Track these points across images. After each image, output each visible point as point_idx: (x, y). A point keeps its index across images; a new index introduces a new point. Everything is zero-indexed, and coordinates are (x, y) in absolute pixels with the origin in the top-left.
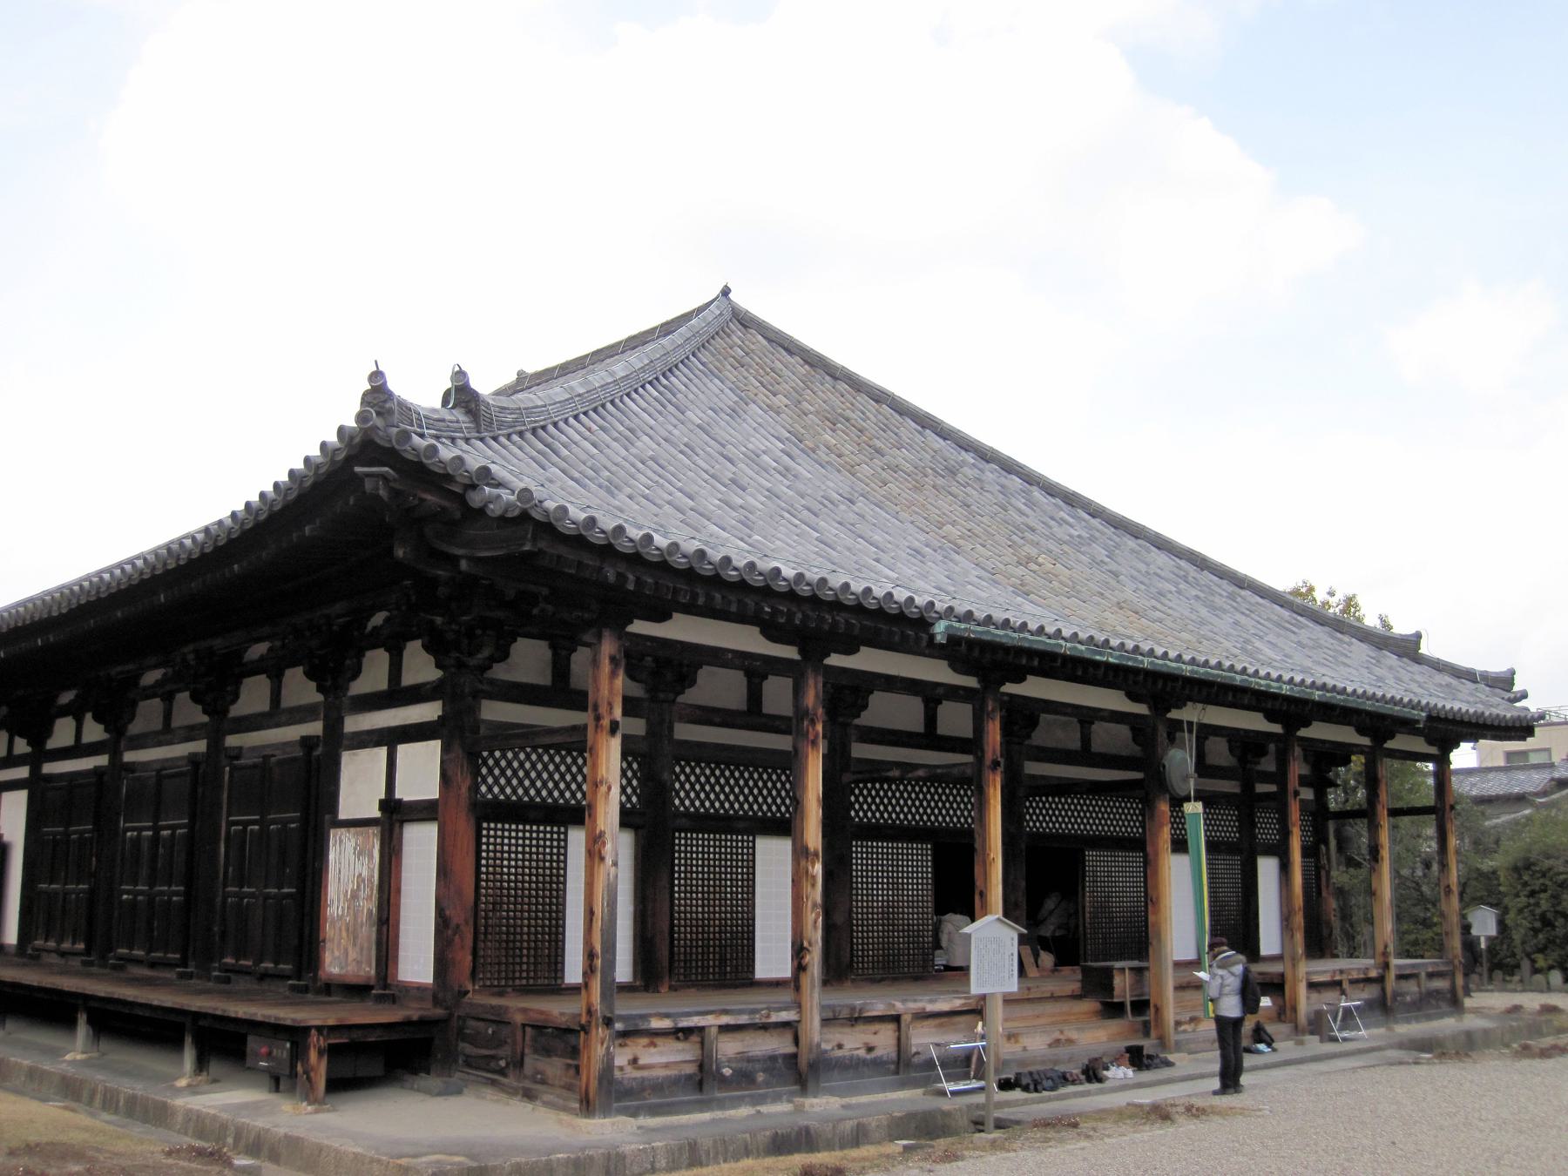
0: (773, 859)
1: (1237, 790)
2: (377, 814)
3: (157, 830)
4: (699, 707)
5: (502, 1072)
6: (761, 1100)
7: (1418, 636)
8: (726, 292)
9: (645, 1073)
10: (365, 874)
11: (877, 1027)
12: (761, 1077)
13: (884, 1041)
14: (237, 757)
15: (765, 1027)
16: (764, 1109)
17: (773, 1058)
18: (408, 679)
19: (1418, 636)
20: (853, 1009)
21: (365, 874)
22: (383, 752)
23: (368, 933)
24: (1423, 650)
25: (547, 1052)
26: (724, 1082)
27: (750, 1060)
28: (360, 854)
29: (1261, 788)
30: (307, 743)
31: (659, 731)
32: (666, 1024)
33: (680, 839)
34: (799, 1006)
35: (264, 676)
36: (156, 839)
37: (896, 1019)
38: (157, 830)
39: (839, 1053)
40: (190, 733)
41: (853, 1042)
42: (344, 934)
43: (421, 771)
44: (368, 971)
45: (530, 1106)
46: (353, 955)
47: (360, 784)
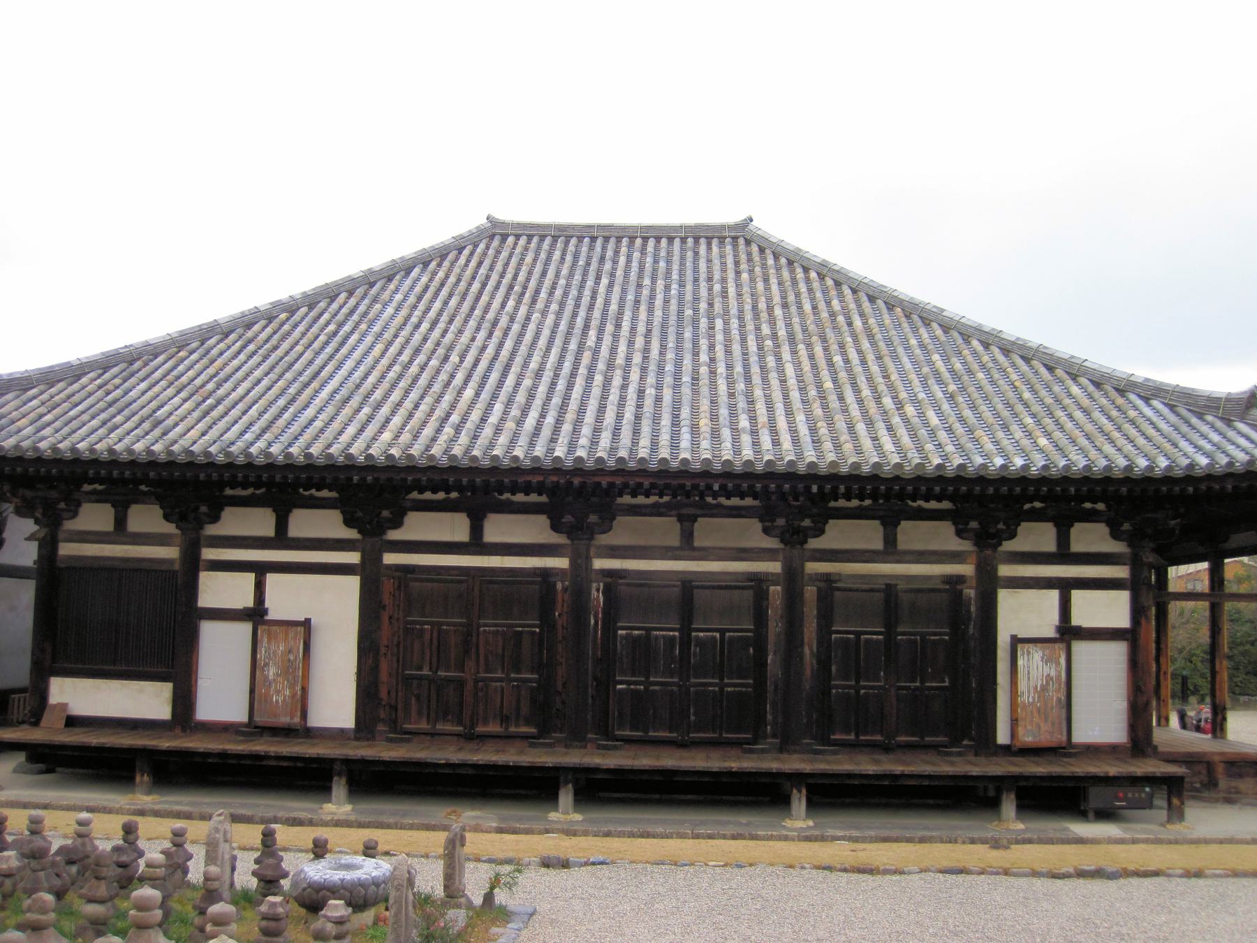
2: (1051, 633)
3: (686, 630)
5: (1197, 790)
10: (1053, 673)
14: (835, 582)
18: (1077, 546)
21: (1053, 673)
22: (1054, 595)
23: (1058, 713)
25: (1241, 776)
28: (1047, 660)
30: (955, 582)
35: (877, 522)
36: (686, 641)
38: (686, 630)
40: (742, 554)
42: (1036, 715)
43: (1107, 609)
44: (1064, 738)
45: (1236, 807)
46: (1044, 727)
47: (1024, 613)
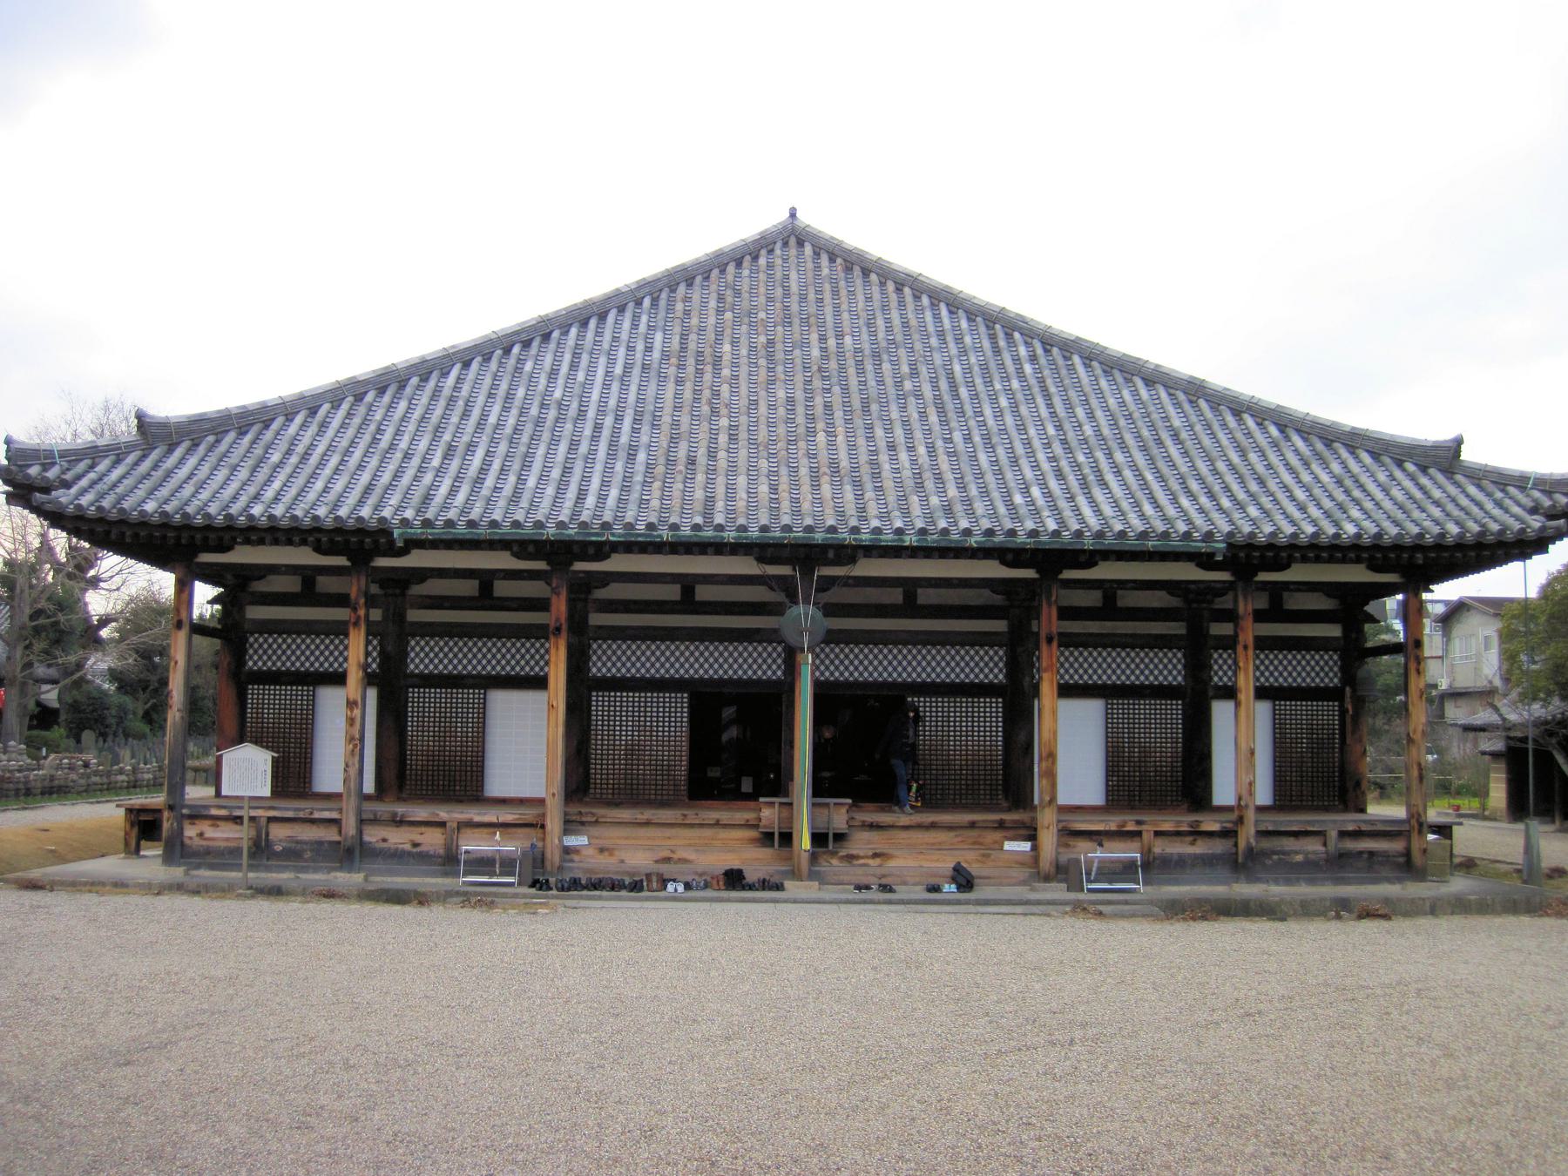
0: (332, 707)
1: (1183, 632)
4: (430, 597)
6: (304, 870)
7: (1459, 442)
8: (793, 214)
9: (210, 843)
11: (423, 829)
12: (308, 855)
13: (432, 840)
15: (313, 821)
16: (302, 876)
17: (320, 843)
19: (1459, 442)
20: (395, 814)
24: (1467, 455)
26: (277, 855)
27: (298, 842)
29: (1220, 629)
31: (400, 618)
32: (223, 812)
33: (413, 694)
34: (340, 811)
37: (442, 824)
39: (385, 845)
41: (398, 838)
